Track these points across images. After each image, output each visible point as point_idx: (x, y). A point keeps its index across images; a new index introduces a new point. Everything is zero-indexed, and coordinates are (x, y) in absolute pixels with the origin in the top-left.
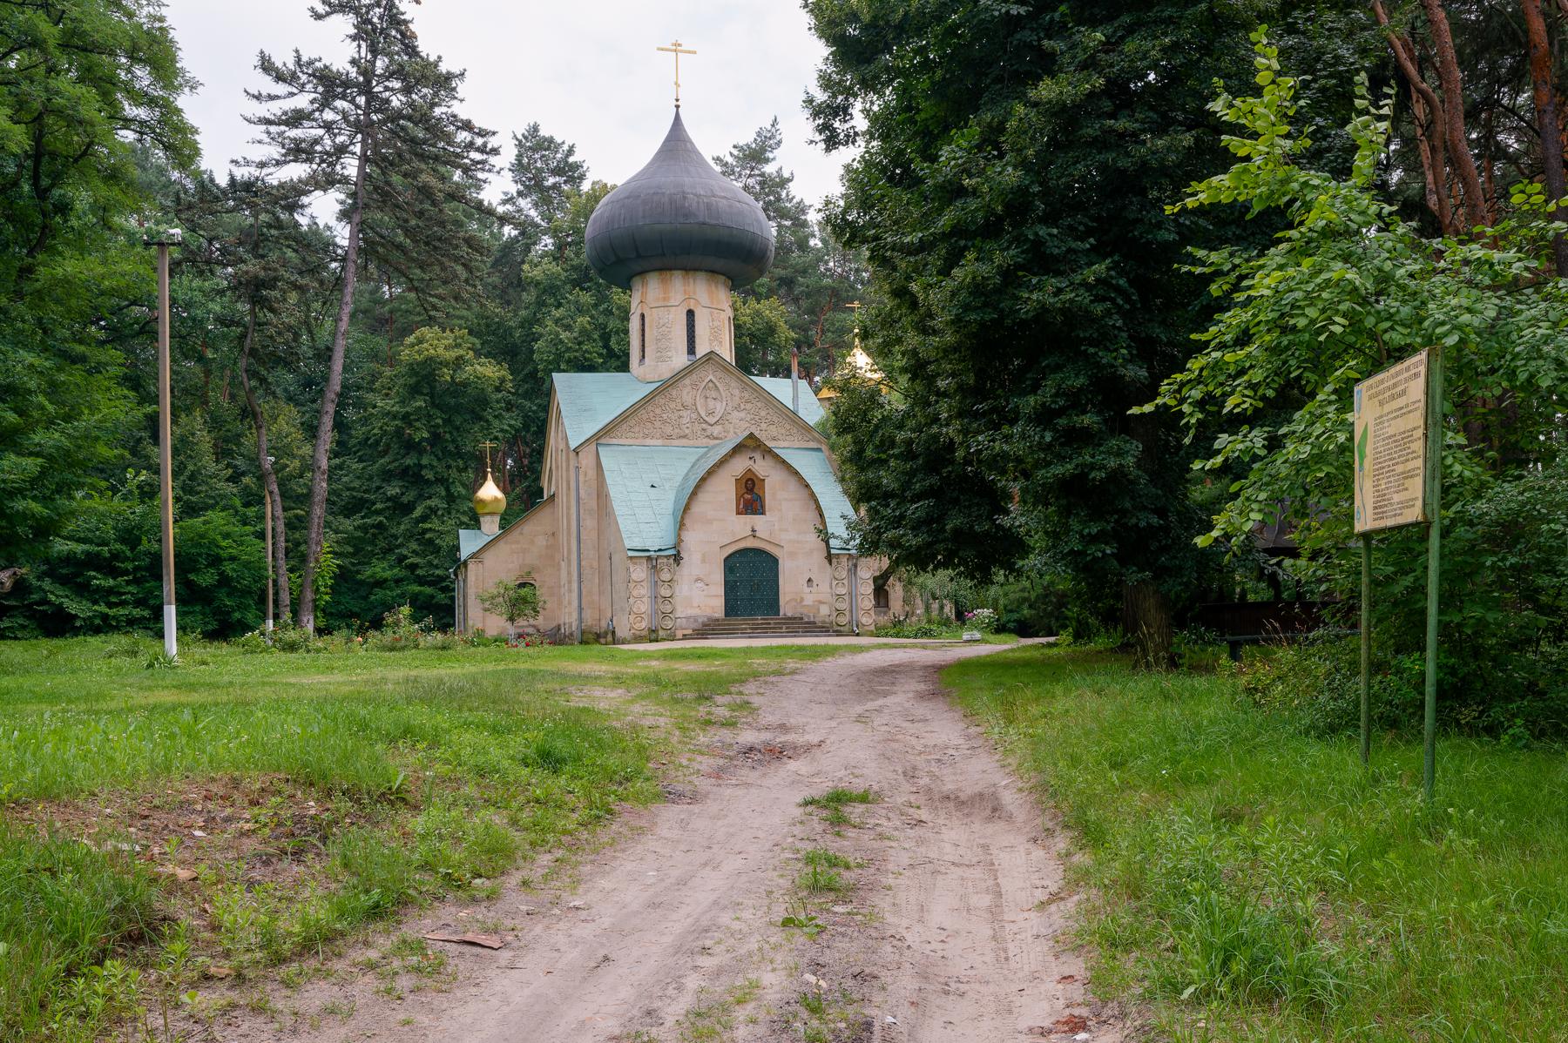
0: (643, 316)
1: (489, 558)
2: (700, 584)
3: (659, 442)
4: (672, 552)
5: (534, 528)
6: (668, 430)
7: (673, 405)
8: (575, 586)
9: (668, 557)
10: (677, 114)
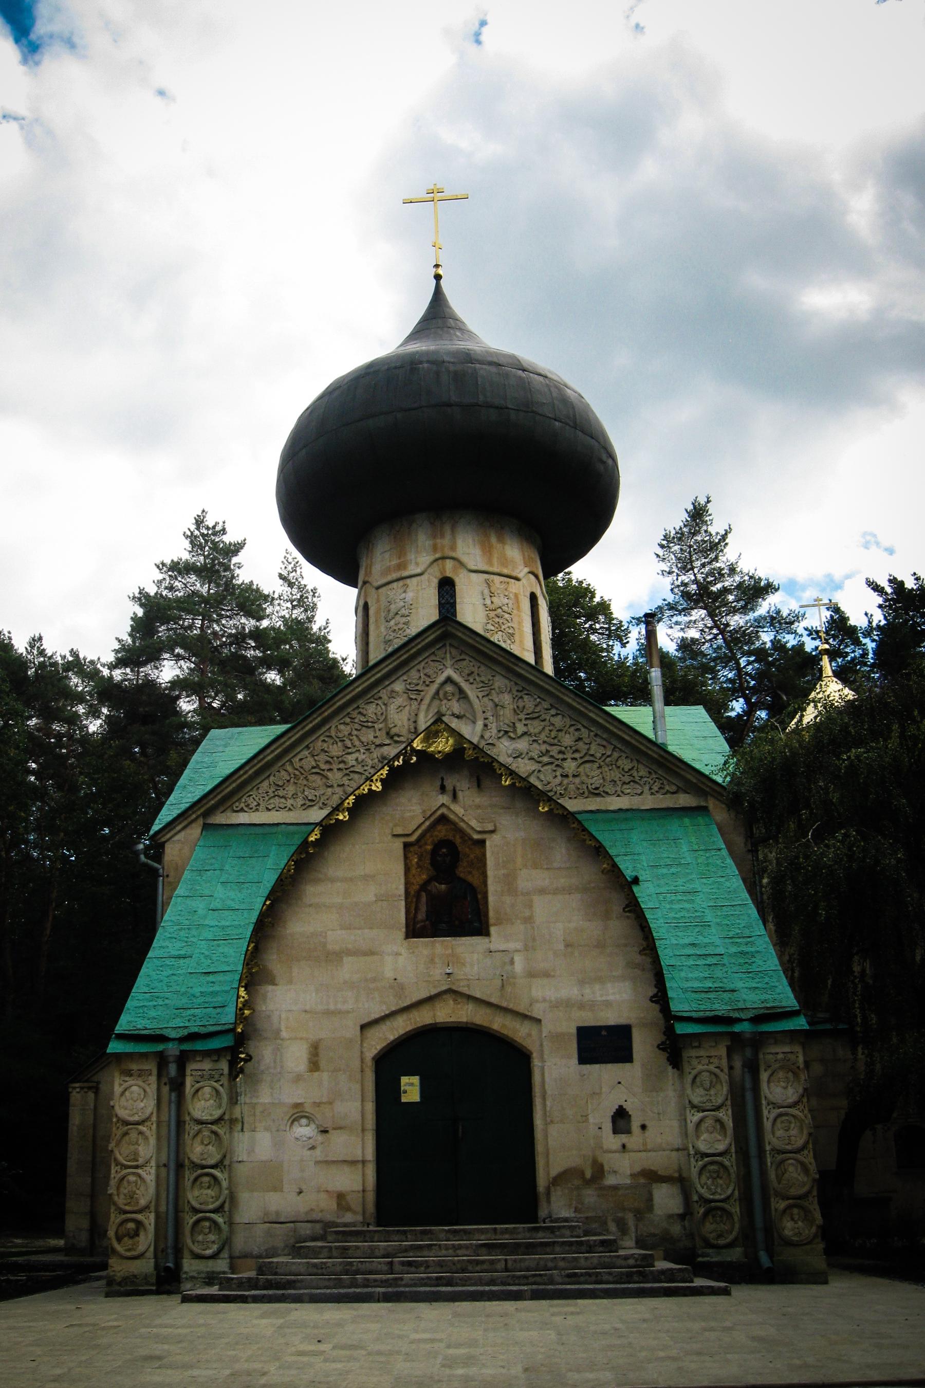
2: (304, 1130)
4: (226, 1041)
9: (207, 1054)
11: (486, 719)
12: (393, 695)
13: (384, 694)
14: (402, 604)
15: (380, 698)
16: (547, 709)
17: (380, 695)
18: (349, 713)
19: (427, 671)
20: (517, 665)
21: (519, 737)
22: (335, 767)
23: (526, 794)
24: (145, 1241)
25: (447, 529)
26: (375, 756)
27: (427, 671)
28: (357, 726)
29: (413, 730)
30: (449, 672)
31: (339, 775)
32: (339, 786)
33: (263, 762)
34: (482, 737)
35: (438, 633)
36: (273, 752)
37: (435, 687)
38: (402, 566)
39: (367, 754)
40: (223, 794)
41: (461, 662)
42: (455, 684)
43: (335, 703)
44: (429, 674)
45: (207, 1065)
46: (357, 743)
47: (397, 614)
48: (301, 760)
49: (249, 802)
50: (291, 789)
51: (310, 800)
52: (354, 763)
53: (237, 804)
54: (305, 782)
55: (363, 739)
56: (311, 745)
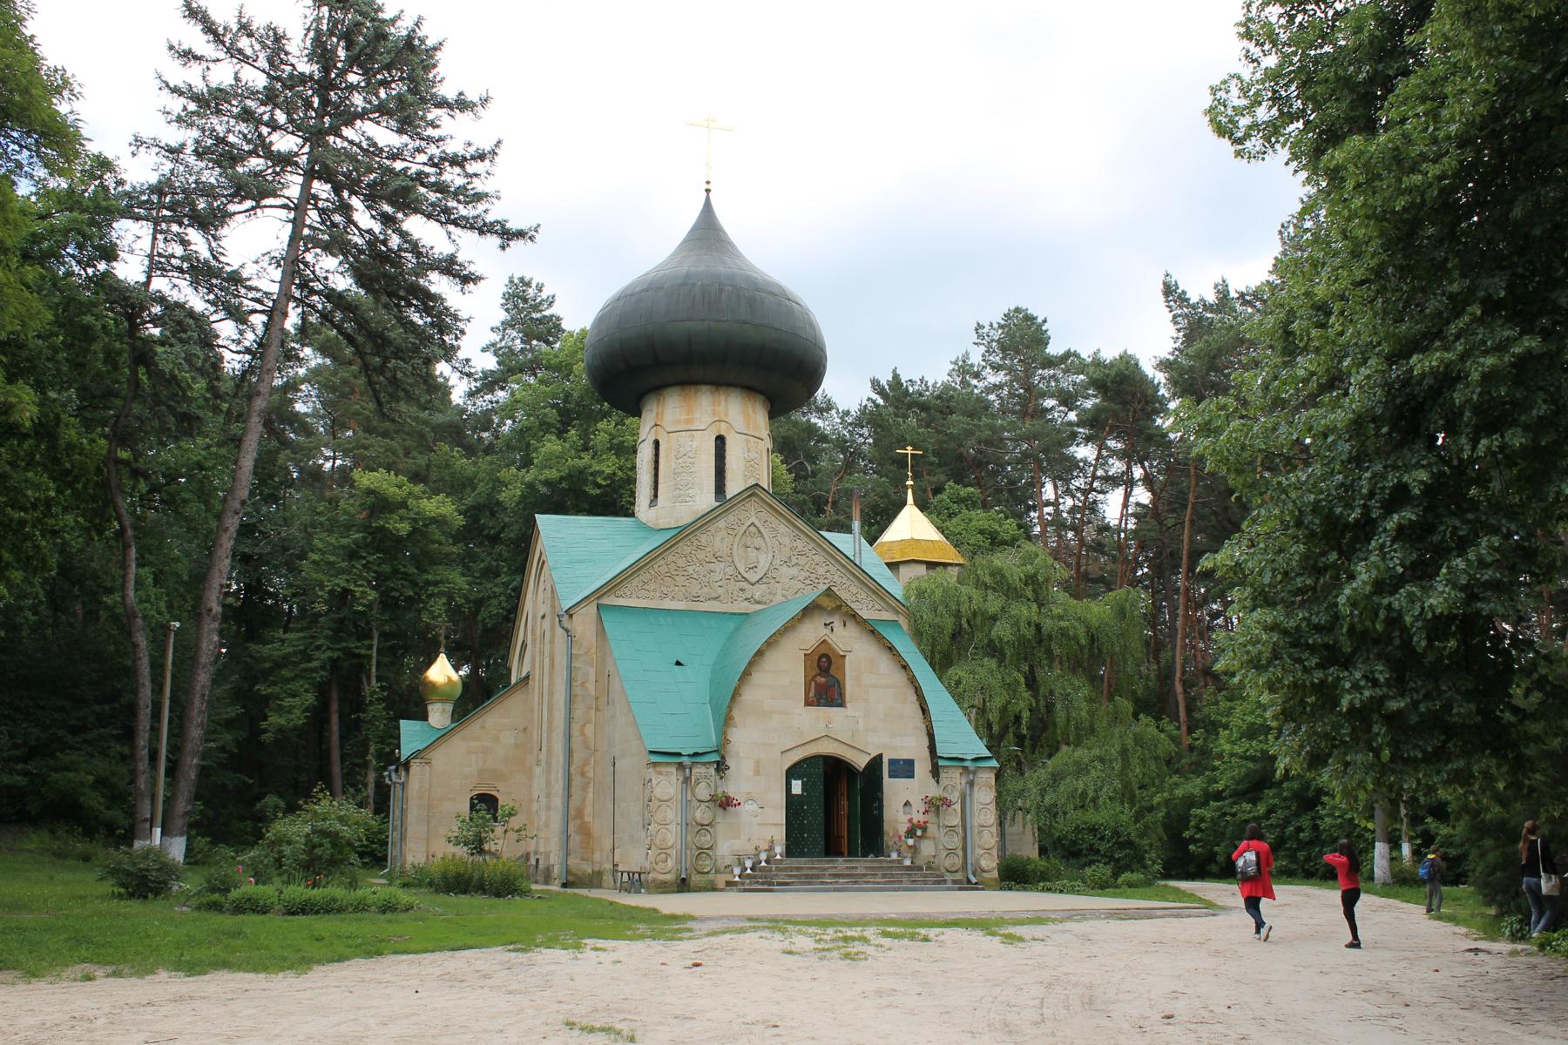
0: (657, 443)
1: (439, 757)
4: (715, 757)
5: (498, 719)
6: (695, 589)
7: (701, 555)
8: (558, 801)
9: (704, 764)
10: (708, 204)
12: (719, 530)
13: (712, 528)
23: (871, 630)
24: (670, 863)
25: (722, 398)
30: (753, 519)
38: (688, 421)
45: (702, 770)
50: (652, 586)
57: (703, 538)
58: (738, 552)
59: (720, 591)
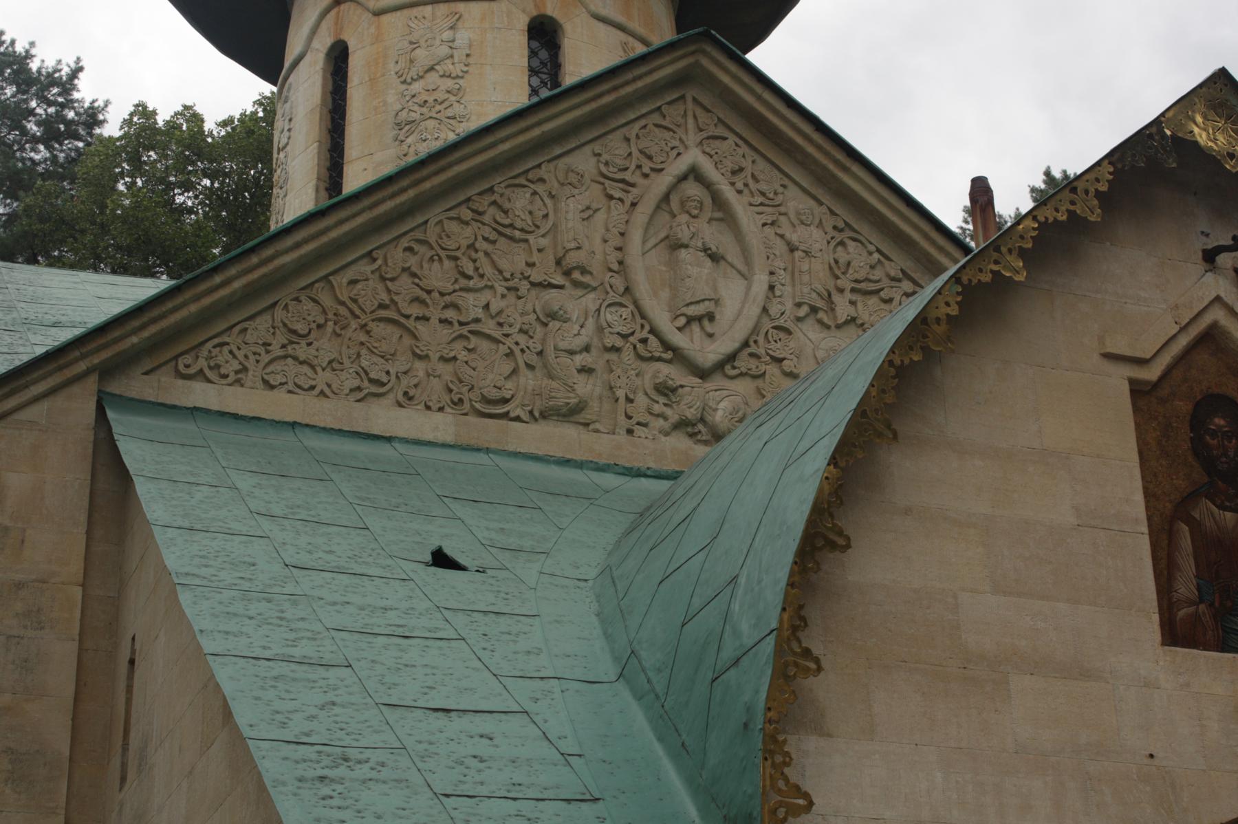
0: (339, 57)
3: (441, 426)
6: (490, 373)
7: (513, 259)
11: (772, 273)
14: (444, 50)
15: (542, 180)
16: (893, 279)
17: (542, 173)
18: (469, 199)
19: (643, 144)
20: (846, 169)
21: (838, 327)
22: (435, 313)
26: (529, 307)
27: (643, 144)
28: (487, 232)
29: (615, 267)
30: (692, 156)
31: (445, 333)
32: (443, 359)
33: (271, 266)
34: (765, 310)
35: (680, 65)
36: (298, 245)
37: (662, 182)
39: (511, 297)
40: (164, 324)
41: (718, 142)
42: (707, 185)
43: (450, 166)
44: (653, 150)
46: (488, 270)
47: (432, 69)
48: (353, 282)
49: (220, 360)
50: (326, 348)
51: (371, 381)
52: (479, 313)
53: (188, 359)
54: (363, 337)
55: (503, 264)
56: (379, 254)
57: (520, 202)
58: (645, 267)
59: (585, 387)
